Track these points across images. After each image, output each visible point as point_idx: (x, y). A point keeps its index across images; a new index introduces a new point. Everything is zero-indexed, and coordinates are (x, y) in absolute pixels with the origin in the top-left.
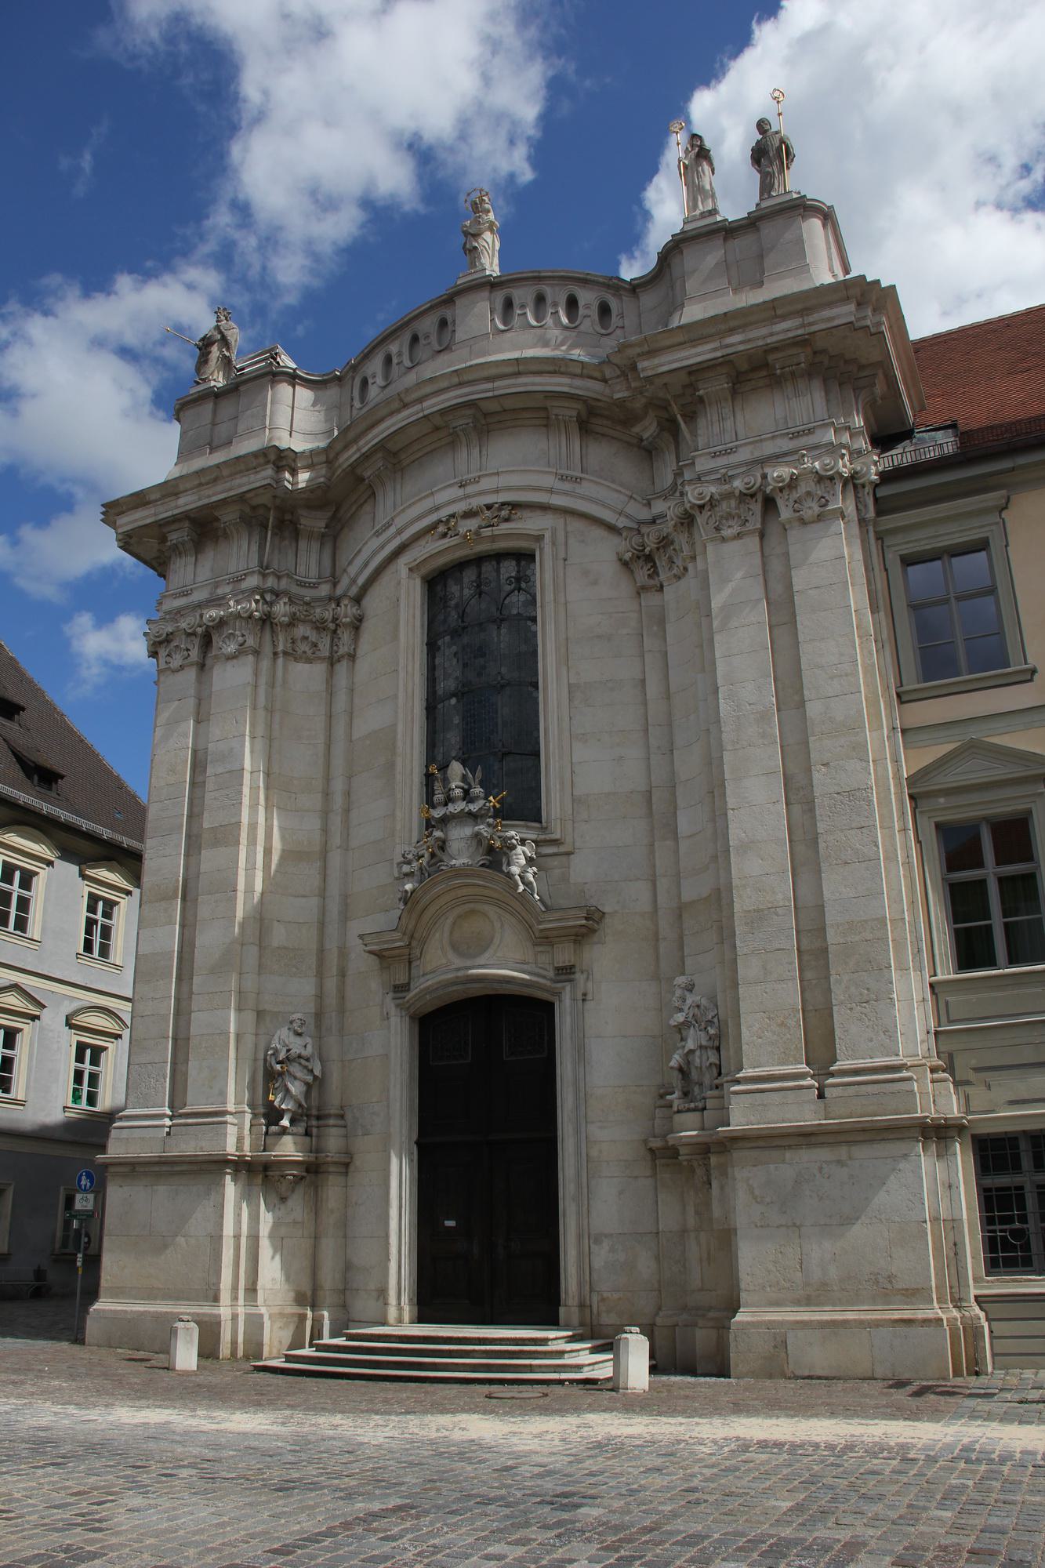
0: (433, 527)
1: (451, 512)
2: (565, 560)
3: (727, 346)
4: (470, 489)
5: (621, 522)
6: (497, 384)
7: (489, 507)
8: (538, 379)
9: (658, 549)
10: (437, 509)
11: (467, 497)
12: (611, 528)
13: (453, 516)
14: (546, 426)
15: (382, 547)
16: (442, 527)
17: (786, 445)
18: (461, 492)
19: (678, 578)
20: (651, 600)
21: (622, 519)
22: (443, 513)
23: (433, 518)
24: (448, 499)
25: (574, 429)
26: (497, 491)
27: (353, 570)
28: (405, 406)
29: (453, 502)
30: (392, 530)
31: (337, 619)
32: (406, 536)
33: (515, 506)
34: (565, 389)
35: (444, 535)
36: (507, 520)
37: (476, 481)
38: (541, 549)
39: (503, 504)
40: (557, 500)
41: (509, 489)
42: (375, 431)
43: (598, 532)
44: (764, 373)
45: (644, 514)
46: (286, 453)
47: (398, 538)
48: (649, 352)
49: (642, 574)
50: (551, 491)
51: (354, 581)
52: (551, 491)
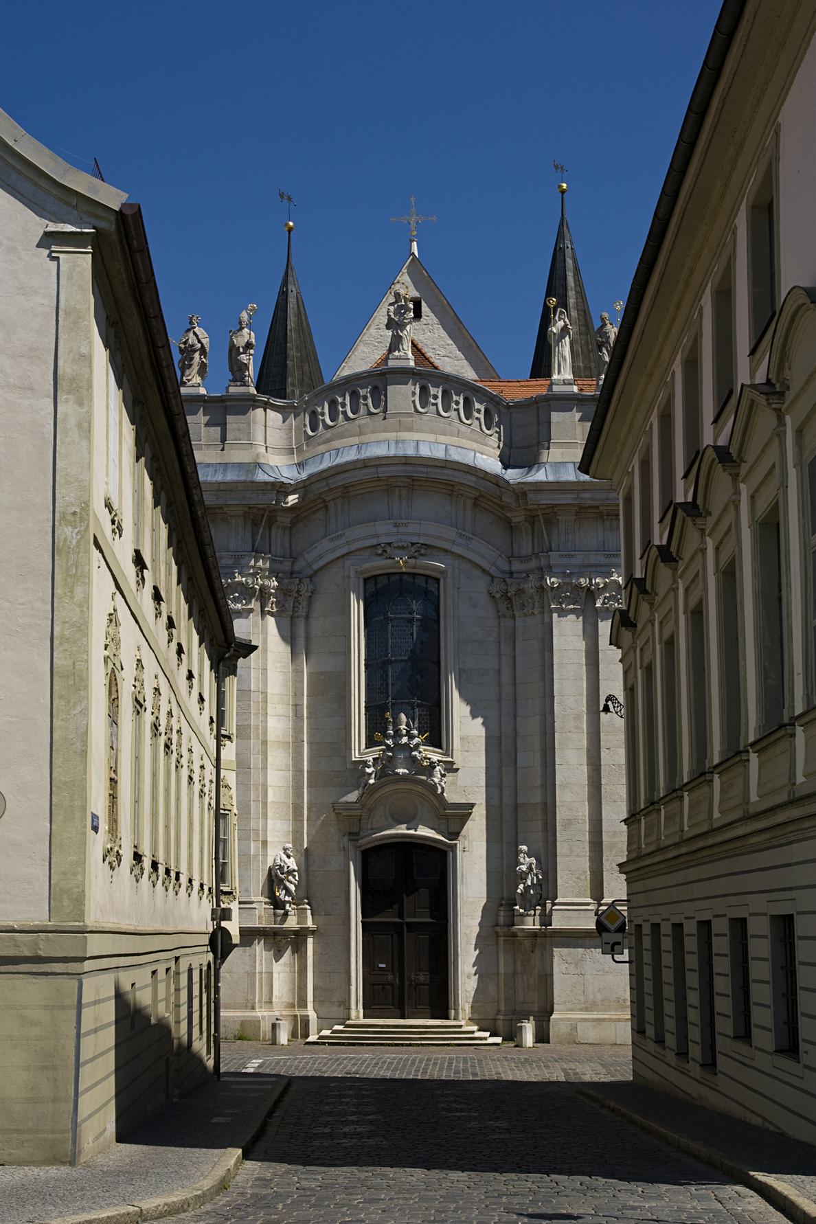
0: (374, 547)
1: (388, 542)
2: (458, 588)
3: (581, 499)
4: (402, 529)
5: (493, 571)
6: (429, 470)
7: (413, 544)
8: (456, 473)
9: (515, 595)
10: (377, 536)
11: (398, 534)
12: (484, 571)
13: (389, 544)
14: (450, 495)
15: (334, 550)
16: (382, 550)
17: (603, 560)
18: (395, 530)
19: (526, 615)
20: (508, 623)
21: (493, 568)
22: (383, 540)
23: (374, 542)
24: (384, 531)
25: (469, 503)
26: (419, 535)
27: (310, 557)
28: (365, 467)
29: (388, 534)
30: (343, 541)
31: (300, 591)
32: (354, 547)
33: (427, 546)
34: (473, 485)
35: (380, 555)
36: (422, 555)
37: (406, 525)
38: (445, 579)
39: (422, 544)
40: (456, 550)
41: (427, 535)
42: (342, 476)
43: (478, 573)
44: (594, 511)
45: (506, 567)
46: (287, 486)
47: (347, 547)
48: (536, 490)
49: (503, 606)
50: (453, 542)
51: (310, 565)
52: (453, 542)
